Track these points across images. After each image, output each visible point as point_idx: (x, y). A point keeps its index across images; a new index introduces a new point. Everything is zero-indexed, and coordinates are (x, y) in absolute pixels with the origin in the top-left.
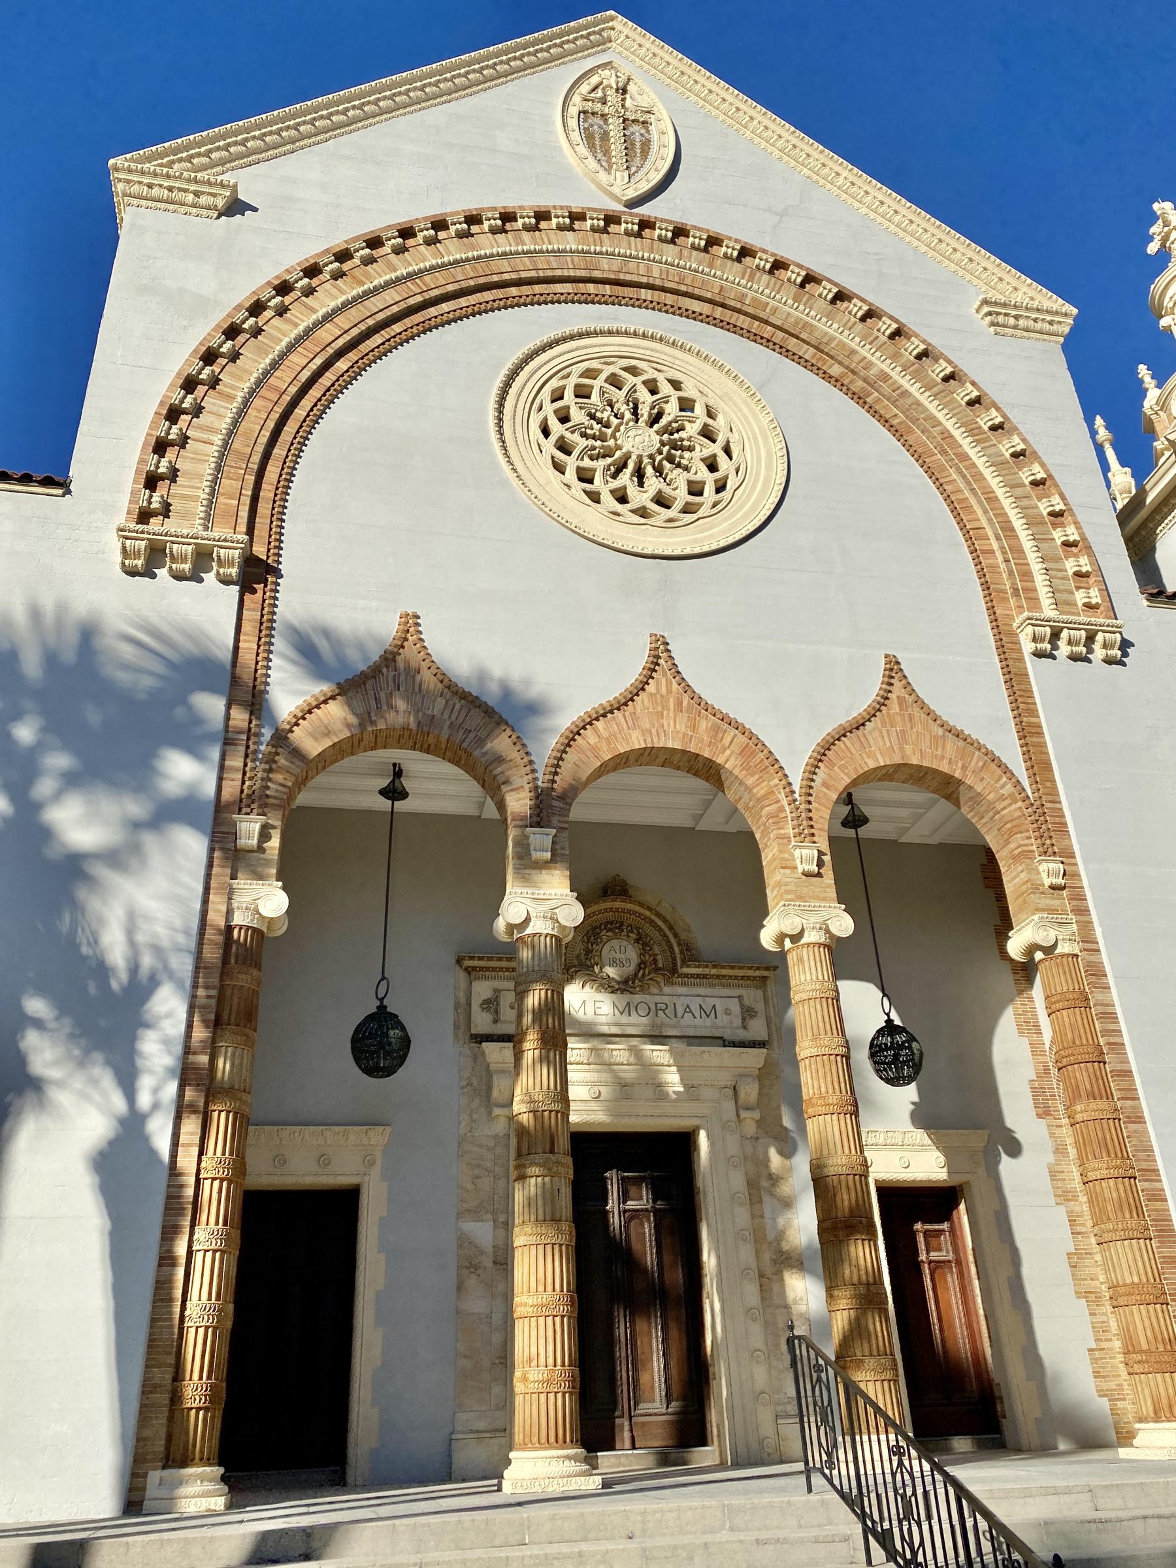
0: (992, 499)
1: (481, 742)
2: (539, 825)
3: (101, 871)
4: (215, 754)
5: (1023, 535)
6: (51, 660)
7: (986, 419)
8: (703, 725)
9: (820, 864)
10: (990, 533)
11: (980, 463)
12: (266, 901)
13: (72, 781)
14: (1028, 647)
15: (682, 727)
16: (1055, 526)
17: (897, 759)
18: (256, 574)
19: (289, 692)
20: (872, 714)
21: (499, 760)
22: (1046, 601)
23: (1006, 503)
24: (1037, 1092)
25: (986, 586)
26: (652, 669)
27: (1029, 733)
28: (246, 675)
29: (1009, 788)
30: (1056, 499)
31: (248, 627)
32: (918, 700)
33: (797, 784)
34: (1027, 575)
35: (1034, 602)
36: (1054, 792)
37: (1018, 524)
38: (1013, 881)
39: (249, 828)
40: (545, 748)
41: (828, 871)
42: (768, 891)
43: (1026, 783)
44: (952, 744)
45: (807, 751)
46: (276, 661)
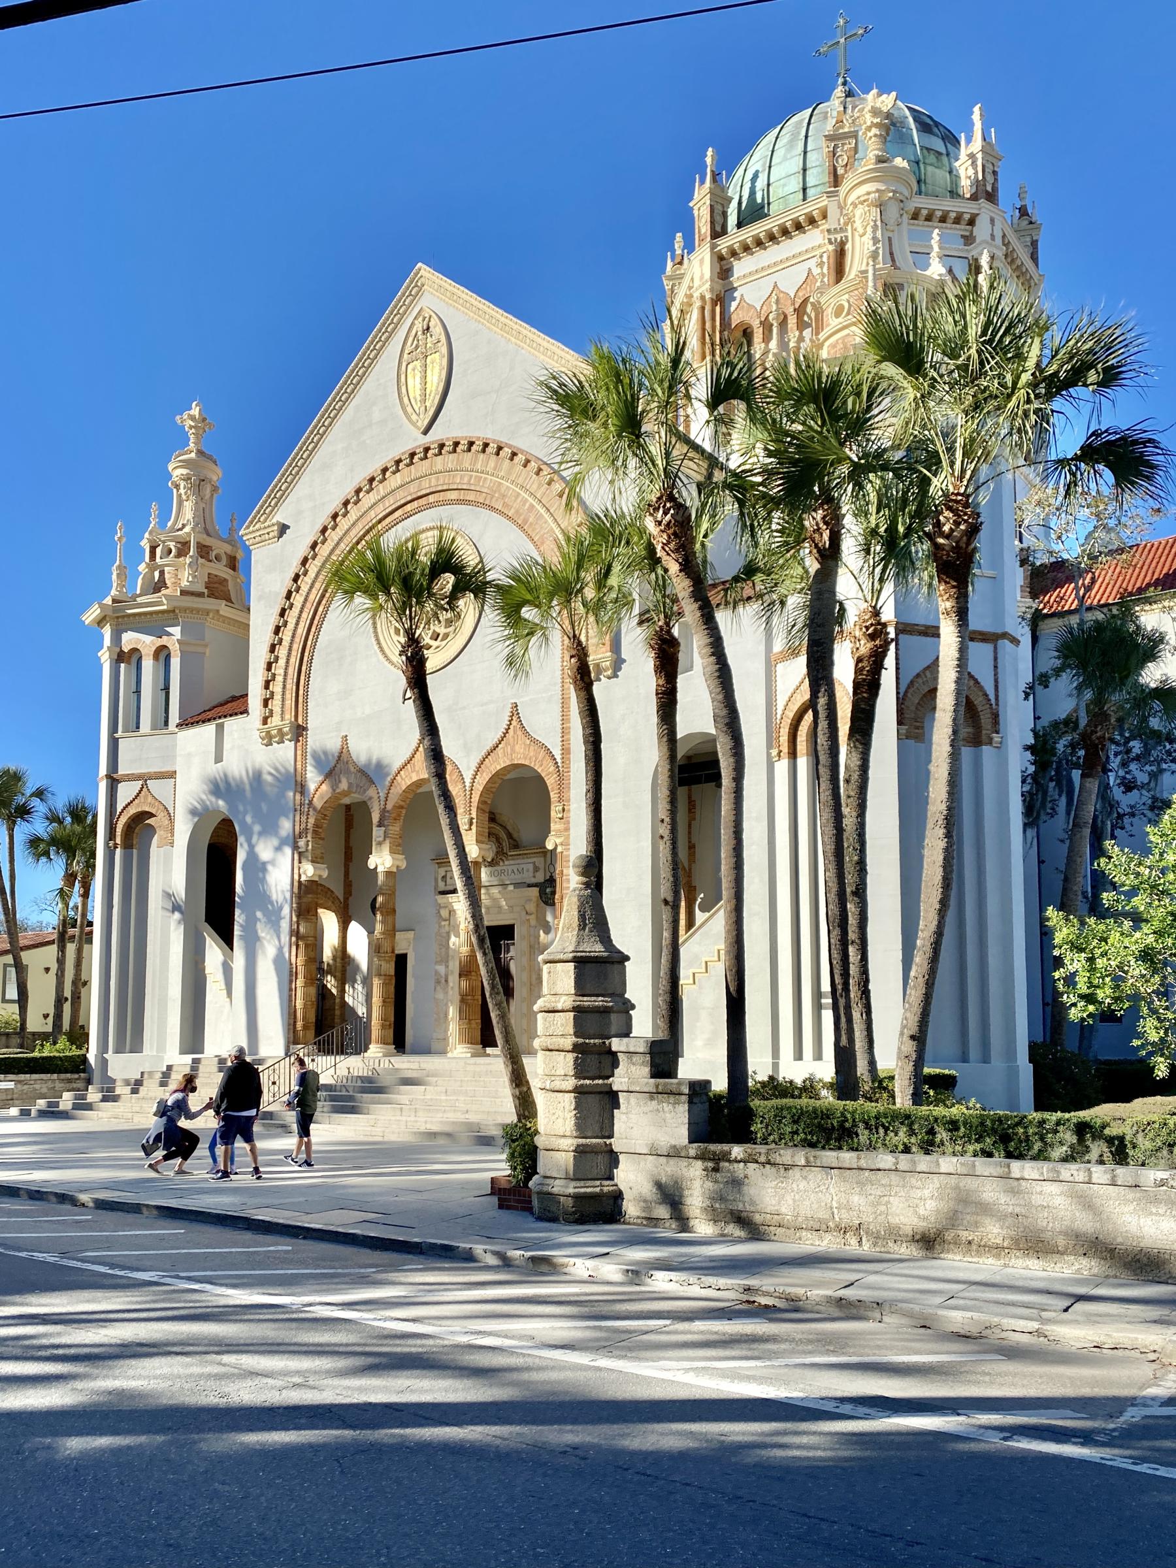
3: (270, 867)
4: (291, 816)
6: (251, 785)
9: (471, 824)
12: (309, 871)
13: (260, 834)
17: (508, 763)
18: (299, 731)
19: (313, 778)
21: (371, 798)
28: (299, 779)
29: (552, 768)
31: (299, 758)
33: (468, 784)
39: (302, 843)
41: (474, 827)
43: (559, 761)
45: (474, 766)
46: (309, 768)
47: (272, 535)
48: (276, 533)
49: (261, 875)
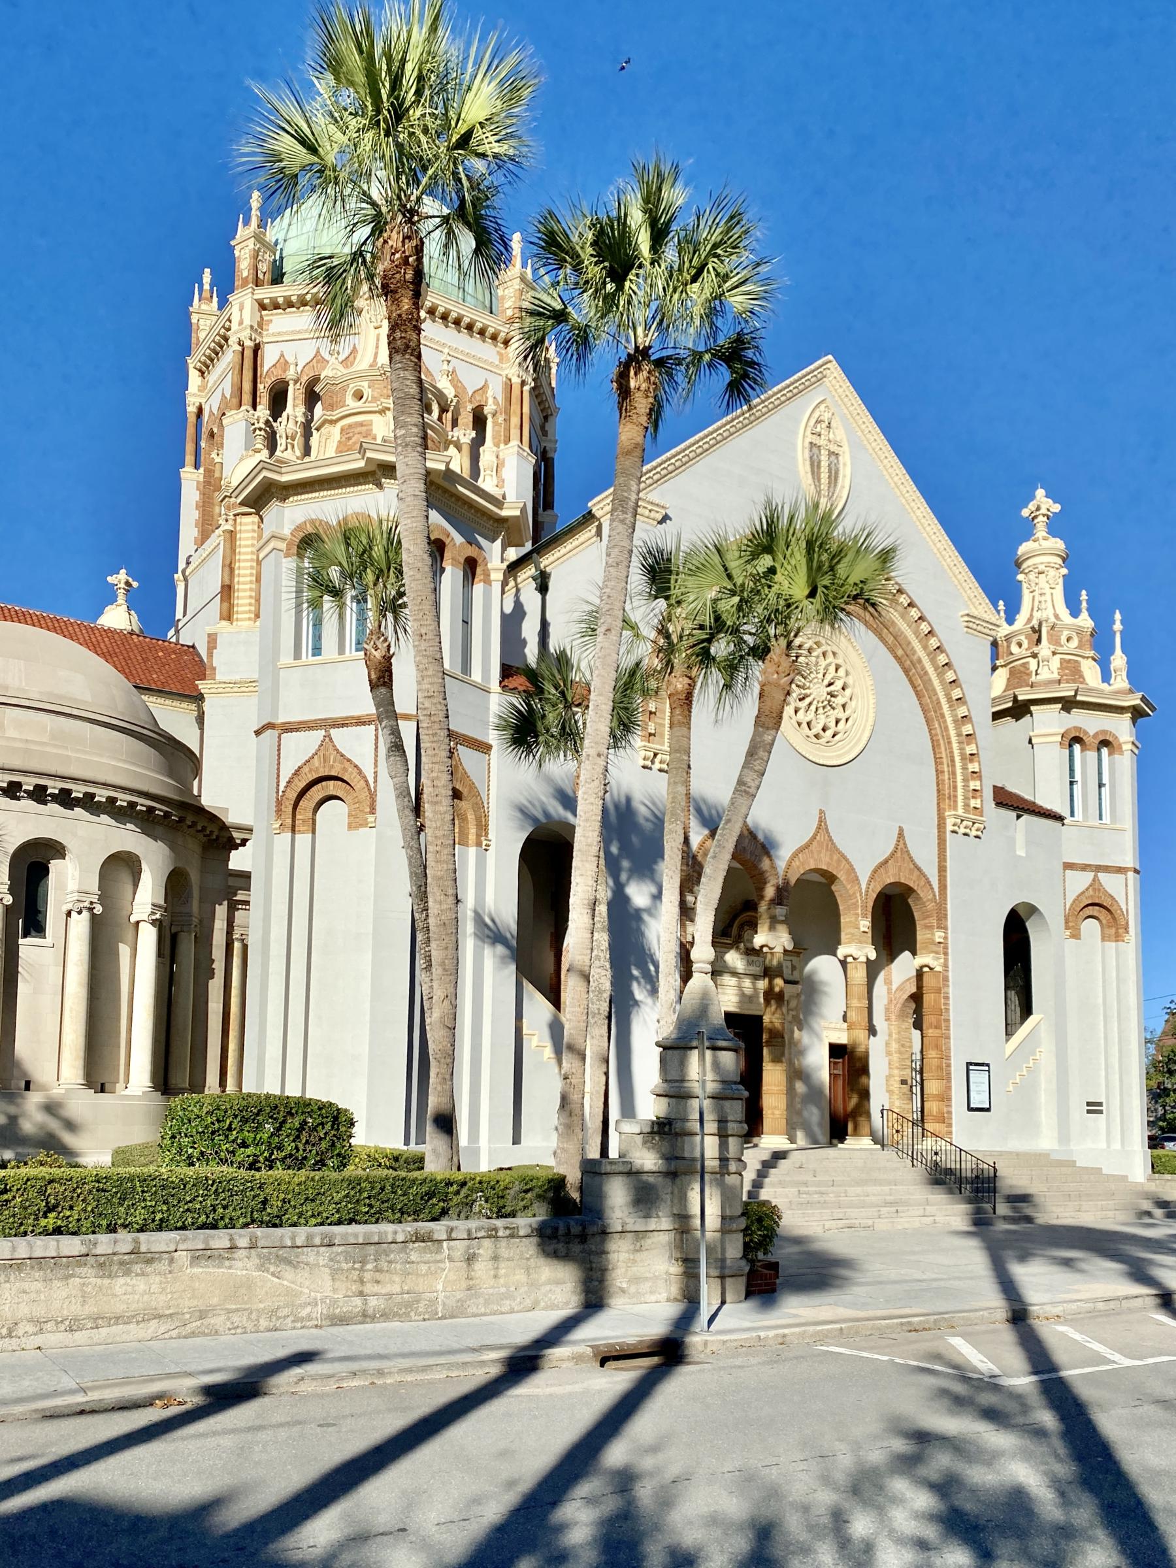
0: (950, 743)
1: (760, 861)
2: (780, 904)
5: (958, 764)
6: (617, 806)
7: (956, 693)
8: (835, 857)
10: (945, 760)
11: (949, 720)
14: (949, 827)
15: (827, 859)
16: (971, 761)
20: (892, 855)
22: (960, 804)
23: (955, 746)
24: (887, 1010)
25: (938, 791)
26: (819, 828)
27: (942, 869)
30: (974, 746)
32: (908, 851)
34: (955, 788)
35: (955, 802)
36: (945, 900)
37: (957, 759)
38: (921, 935)
40: (781, 865)
42: (843, 934)
44: (916, 873)
47: (653, 514)
48: (659, 517)
49: (634, 924)
